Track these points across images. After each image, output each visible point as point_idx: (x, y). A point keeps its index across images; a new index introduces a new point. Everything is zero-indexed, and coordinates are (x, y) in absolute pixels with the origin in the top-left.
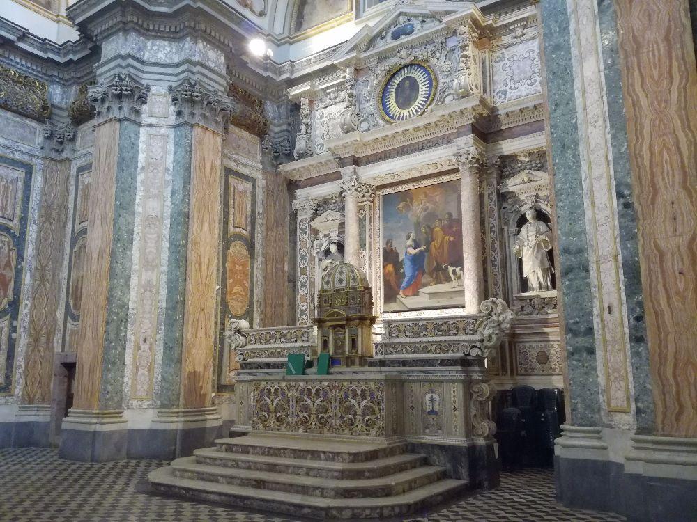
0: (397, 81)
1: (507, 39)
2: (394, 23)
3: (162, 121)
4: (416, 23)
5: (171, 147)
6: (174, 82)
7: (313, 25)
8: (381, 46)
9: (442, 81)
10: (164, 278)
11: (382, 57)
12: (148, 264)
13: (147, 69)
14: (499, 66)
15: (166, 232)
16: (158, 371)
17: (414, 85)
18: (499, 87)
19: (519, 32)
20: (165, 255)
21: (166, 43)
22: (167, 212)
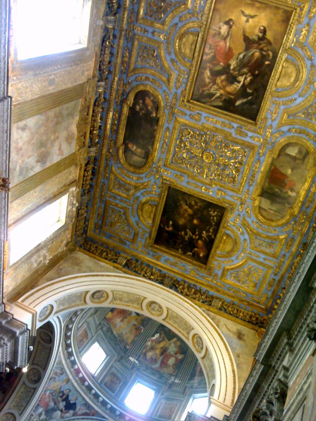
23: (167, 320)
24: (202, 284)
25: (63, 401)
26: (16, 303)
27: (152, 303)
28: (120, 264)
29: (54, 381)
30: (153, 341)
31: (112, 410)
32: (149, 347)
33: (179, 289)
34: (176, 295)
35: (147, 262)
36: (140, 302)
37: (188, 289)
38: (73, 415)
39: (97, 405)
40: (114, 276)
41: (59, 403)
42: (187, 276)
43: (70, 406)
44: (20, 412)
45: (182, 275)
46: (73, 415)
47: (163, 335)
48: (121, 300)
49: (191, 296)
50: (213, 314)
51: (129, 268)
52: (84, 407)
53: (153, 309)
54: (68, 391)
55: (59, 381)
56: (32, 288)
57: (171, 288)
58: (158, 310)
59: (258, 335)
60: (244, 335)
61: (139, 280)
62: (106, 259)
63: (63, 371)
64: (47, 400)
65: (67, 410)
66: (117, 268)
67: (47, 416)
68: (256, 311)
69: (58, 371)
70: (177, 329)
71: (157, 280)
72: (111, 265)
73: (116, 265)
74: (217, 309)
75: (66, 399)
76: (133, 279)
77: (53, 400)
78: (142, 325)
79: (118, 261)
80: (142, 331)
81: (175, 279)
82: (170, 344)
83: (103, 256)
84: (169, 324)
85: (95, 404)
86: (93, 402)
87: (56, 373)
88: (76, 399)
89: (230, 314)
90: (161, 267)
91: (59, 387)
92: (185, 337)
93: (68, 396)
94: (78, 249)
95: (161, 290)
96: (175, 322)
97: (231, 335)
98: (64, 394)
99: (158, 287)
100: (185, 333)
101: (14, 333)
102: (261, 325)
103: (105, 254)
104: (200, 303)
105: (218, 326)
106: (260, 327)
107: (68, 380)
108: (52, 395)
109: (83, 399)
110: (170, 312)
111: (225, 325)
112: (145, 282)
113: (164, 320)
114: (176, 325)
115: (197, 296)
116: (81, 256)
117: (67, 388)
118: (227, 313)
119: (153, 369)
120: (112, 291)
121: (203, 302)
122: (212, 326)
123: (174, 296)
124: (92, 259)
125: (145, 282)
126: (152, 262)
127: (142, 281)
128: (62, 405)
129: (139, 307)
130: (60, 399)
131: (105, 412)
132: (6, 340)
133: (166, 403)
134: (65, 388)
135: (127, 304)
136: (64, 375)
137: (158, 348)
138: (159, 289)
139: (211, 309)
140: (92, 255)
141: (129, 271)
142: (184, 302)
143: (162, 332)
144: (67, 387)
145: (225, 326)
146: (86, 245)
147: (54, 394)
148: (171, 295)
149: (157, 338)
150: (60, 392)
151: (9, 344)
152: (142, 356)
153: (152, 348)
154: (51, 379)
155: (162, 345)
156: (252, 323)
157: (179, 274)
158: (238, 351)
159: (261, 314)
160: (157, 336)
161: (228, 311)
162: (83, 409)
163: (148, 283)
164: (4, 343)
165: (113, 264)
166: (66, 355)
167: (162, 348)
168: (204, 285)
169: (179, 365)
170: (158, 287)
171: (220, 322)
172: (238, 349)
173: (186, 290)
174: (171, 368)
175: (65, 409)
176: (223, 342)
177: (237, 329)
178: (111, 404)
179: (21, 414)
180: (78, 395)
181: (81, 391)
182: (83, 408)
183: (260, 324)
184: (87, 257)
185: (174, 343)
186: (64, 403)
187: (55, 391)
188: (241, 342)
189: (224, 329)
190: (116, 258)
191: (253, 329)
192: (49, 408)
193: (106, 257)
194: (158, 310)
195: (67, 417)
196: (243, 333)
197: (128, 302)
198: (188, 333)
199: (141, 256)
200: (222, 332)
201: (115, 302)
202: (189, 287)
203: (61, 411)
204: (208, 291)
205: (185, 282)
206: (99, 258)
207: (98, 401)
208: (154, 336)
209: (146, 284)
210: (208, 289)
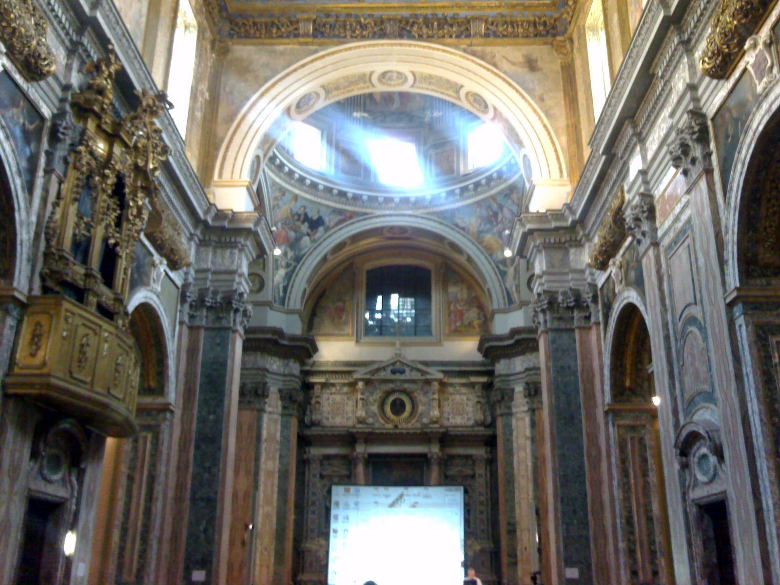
0: (392, 398)
1: (451, 390)
2: (394, 364)
3: (275, 410)
4: (407, 370)
5: (279, 427)
6: (280, 385)
7: (322, 332)
8: (382, 375)
9: (421, 408)
10: (275, 511)
11: (385, 381)
12: (268, 502)
13: (269, 375)
14: (446, 403)
15: (276, 482)
16: (272, 568)
17: (403, 405)
18: (446, 415)
19: (458, 388)
20: (275, 496)
21: (277, 359)
22: (277, 469)
23: (417, 84)
24: (443, 7)
25: (303, 222)
26: (212, 183)
27: (384, 75)
28: (306, 35)
29: (279, 208)
31: (373, 199)
33: (413, 33)
34: (415, 46)
35: (347, 11)
37: (427, 27)
39: (349, 205)
40: (312, 61)
42: (415, 5)
43: (315, 224)
44: (261, 266)
45: (407, 7)
48: (337, 88)
49: (436, 36)
50: (479, 49)
51: (322, 34)
56: (217, 149)
57: (401, 36)
58: (398, 78)
59: (556, 50)
60: (536, 61)
61: (350, 49)
62: (281, 37)
63: (283, 191)
64: (284, 233)
66: (306, 44)
68: (538, 13)
69: (277, 194)
70: (437, 92)
71: (375, 33)
72: (294, 44)
73: (301, 40)
74: (481, 36)
75: (306, 218)
76: (340, 51)
79: (301, 32)
81: (399, 17)
83: (274, 35)
84: (422, 88)
85: (346, 204)
86: (343, 203)
87: (276, 199)
88: (319, 212)
89: (504, 36)
90: (370, 8)
92: (454, 97)
93: (306, 215)
94: (230, 43)
95: (389, 48)
96: (430, 83)
97: (520, 70)
98: (299, 216)
99: (382, 45)
101: (249, 231)
102: (554, 32)
103: (274, 31)
104: (453, 40)
105: (495, 65)
106: (554, 36)
107: (296, 197)
109: (328, 207)
110: (417, 76)
111: (504, 57)
112: (359, 47)
113: (412, 86)
115: (445, 31)
116: (243, 50)
118: (498, 36)
120: (323, 87)
121: (458, 37)
122: (488, 70)
123: (413, 48)
124: (260, 47)
125: (359, 47)
126: (353, 8)
127: (356, 48)
128: (305, 228)
129: (368, 84)
130: (298, 223)
131: (363, 207)
132: (242, 240)
133: (436, 154)
134: (297, 207)
138: (385, 47)
139: (475, 41)
140: (255, 41)
141: (327, 40)
142: (431, 51)
144: (299, 204)
145: (504, 60)
146: (236, 29)
148: (408, 48)
150: (293, 216)
151: (248, 243)
152: (368, 102)
154: (274, 208)
156: (541, 36)
157: (402, 7)
158: (539, 91)
159: (548, 13)
161: (498, 33)
163: (364, 46)
164: (242, 245)
165: (295, 40)
166: (287, 179)
168: (448, 7)
170: (382, 45)
171: (495, 56)
172: (537, 88)
173: (425, 30)
176: (514, 88)
177: (524, 56)
178: (365, 194)
179: (264, 269)
181: (319, 200)
183: (551, 31)
184: (251, 48)
186: (306, 224)
187: (287, 218)
188: (538, 75)
189: (506, 66)
190: (295, 26)
191: (545, 44)
192: (292, 240)
193: (279, 33)
194: (398, 78)
195: (319, 238)
196: (534, 57)
197: (349, 86)
198: (458, 92)
199: (331, 6)
200: (505, 73)
201: (330, 95)
202: (427, 22)
203: (308, 235)
204: (458, 15)
205: (416, 16)
206: (269, 41)
207: (347, 199)
209: (362, 49)
210: (457, 11)
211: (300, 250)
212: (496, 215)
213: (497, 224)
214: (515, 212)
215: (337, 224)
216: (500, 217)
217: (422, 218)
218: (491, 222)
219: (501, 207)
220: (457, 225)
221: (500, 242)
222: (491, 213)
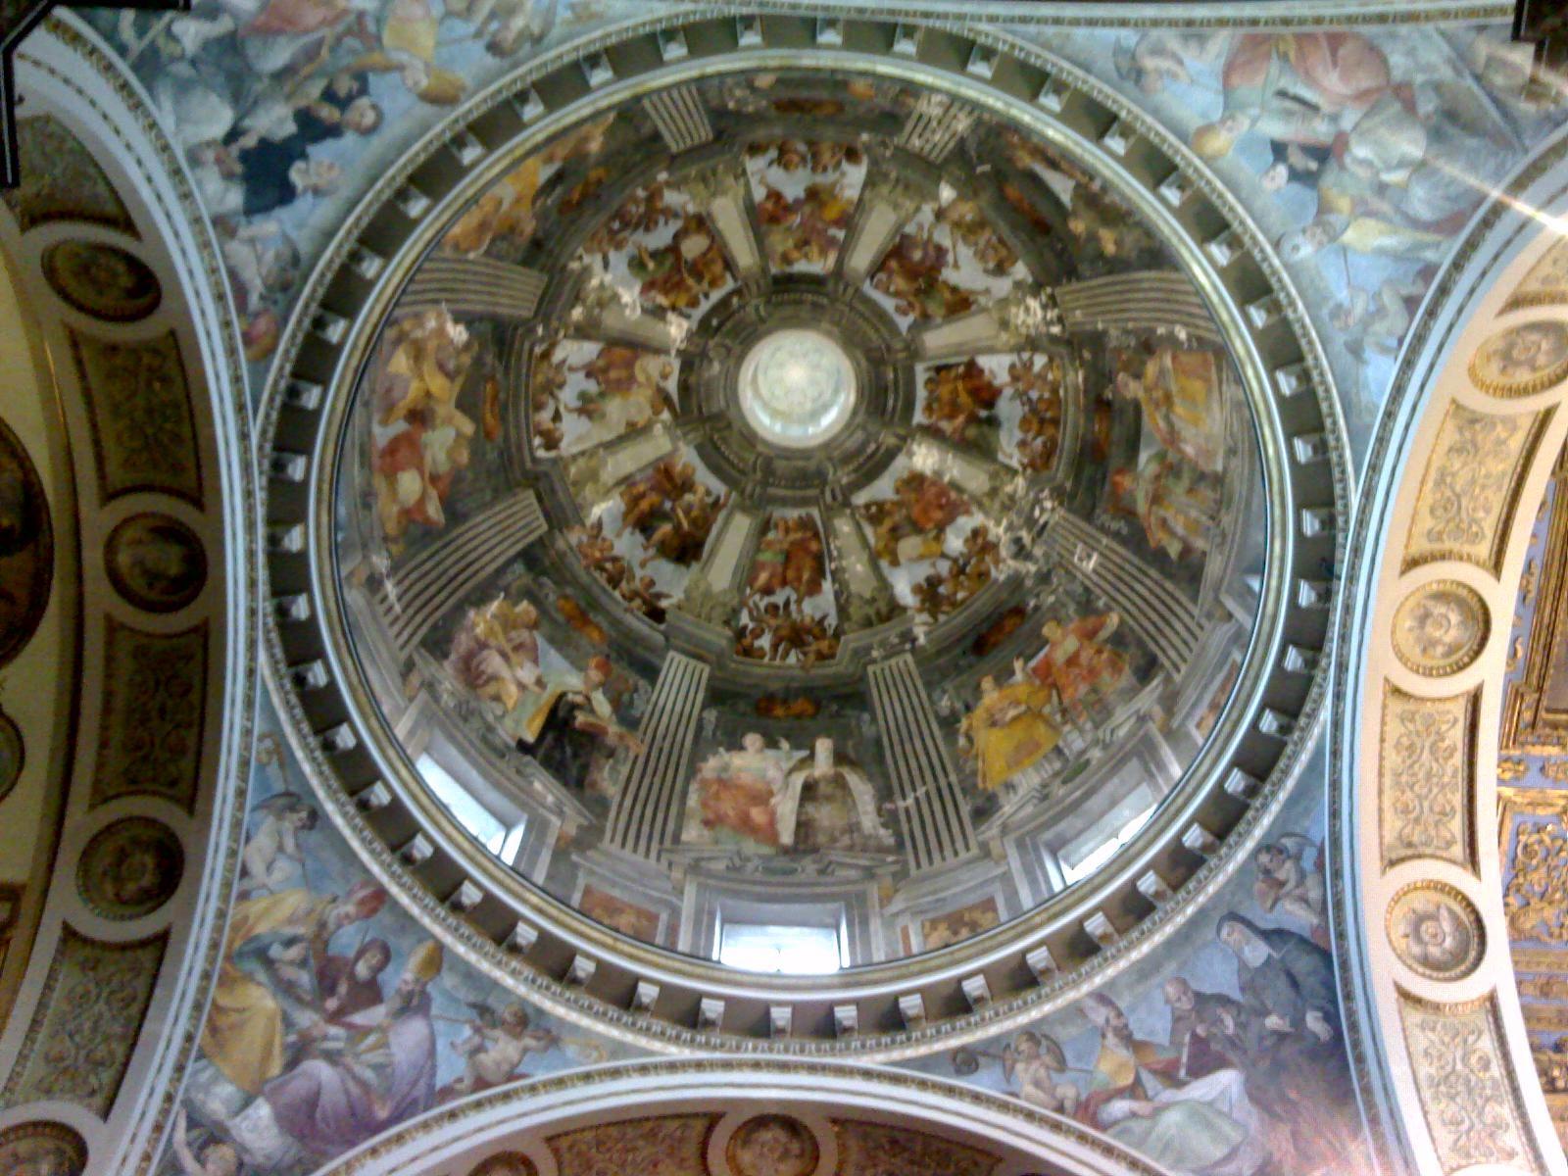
23: (1397, 706)
29: (449, 14)
30: (441, 332)
32: (418, 334)
36: (1448, 544)
38: (218, 221)
41: (289, 97)
43: (266, 175)
46: (218, 221)
47: (466, 360)
48: (1455, 450)
52: (278, 256)
53: (1424, 618)
54: (369, 118)
55: (438, 44)
65: (238, 168)
67: (193, 62)
69: (518, 23)
75: (312, 128)
77: (311, 53)
78: (493, 241)
80: (471, 256)
82: (449, 421)
88: (317, 191)
91: (404, 58)
93: (334, 131)
98: (343, 103)
100: (1393, 824)
108: (349, 32)
109: (329, 235)
114: (1393, 759)
117: (386, 105)
119: (370, 433)
128: (275, 121)
129: (1420, 546)
130: (315, 89)
135: (1430, 484)
136: (491, 61)
137: (421, 377)
143: (476, 347)
147: (351, 42)
149: (452, 342)
153: (418, 354)
155: (437, 384)
160: (458, 333)
162: (259, 259)
167: (428, 394)
169: (416, 533)
174: (395, 509)
175: (245, 156)
180: (346, 192)
182: (270, 255)
185: (459, 435)
192: (252, 48)
197: (1440, 482)
201: (1450, 425)
203: (234, 134)
208: (456, 321)
211: (183, 88)
212: (369, 993)
213: (335, 1017)
214: (443, 1078)
215: (233, 274)
216: (376, 1015)
217: (251, 673)
218: (326, 983)
219: (414, 1004)
220: (248, 839)
221: (275, 1068)
222: (362, 970)
